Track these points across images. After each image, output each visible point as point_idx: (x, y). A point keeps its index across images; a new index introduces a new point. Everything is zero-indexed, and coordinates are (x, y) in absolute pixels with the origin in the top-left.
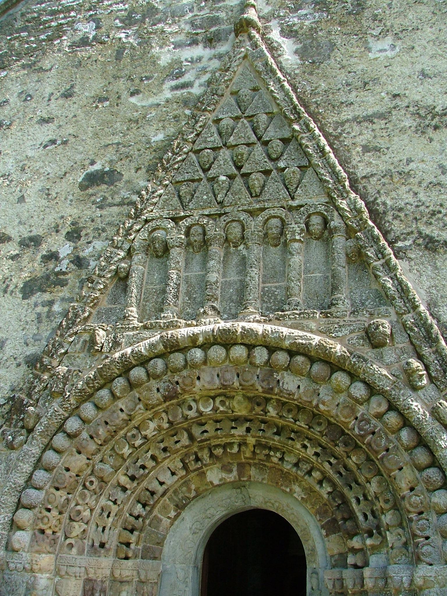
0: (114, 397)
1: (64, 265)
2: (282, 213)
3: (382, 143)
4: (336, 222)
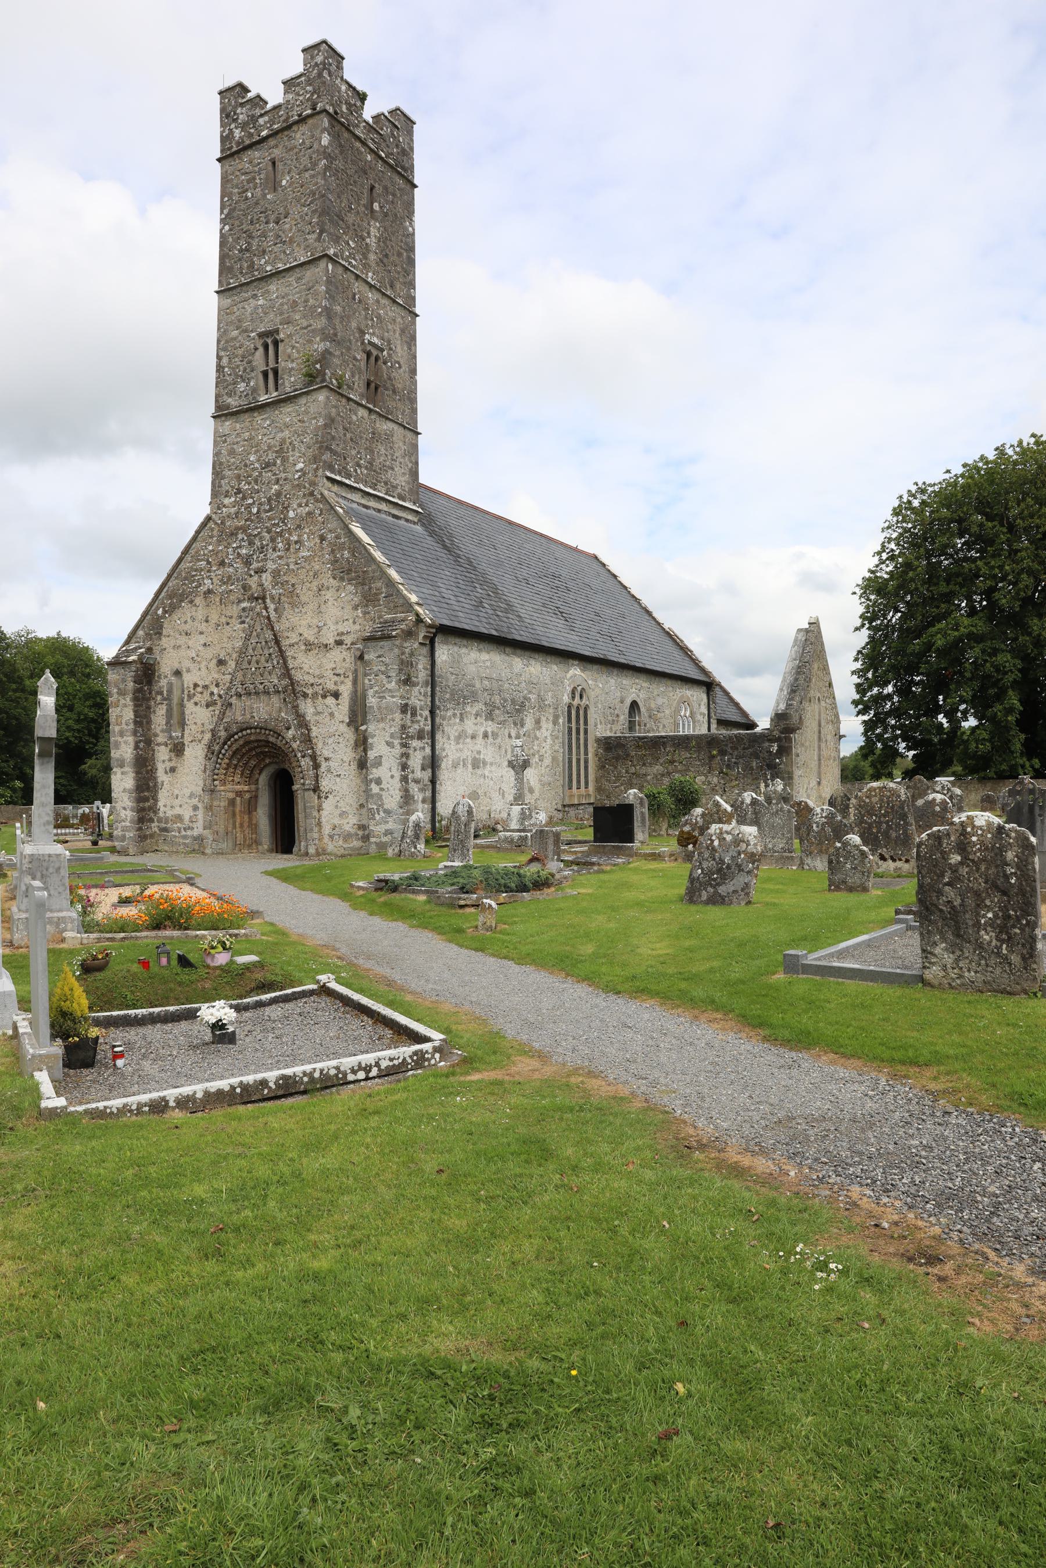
1: (216, 697)
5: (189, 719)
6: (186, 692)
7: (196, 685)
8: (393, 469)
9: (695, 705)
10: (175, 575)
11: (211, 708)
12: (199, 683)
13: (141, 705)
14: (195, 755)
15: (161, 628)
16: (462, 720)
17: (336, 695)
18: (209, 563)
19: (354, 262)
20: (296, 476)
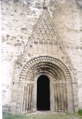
0: (33, 62)
2: (52, 40)
3: (63, 32)
4: (58, 43)
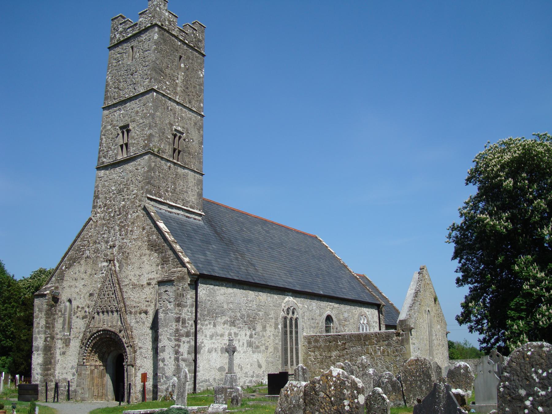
1: (87, 314)
5: (74, 325)
6: (73, 311)
7: (78, 307)
8: (187, 193)
9: (370, 317)
10: (72, 248)
11: (85, 320)
12: (80, 306)
13: (50, 318)
14: (75, 344)
15: (64, 277)
16: (215, 325)
17: (146, 312)
18: (88, 242)
19: (168, 92)
20: (133, 197)
